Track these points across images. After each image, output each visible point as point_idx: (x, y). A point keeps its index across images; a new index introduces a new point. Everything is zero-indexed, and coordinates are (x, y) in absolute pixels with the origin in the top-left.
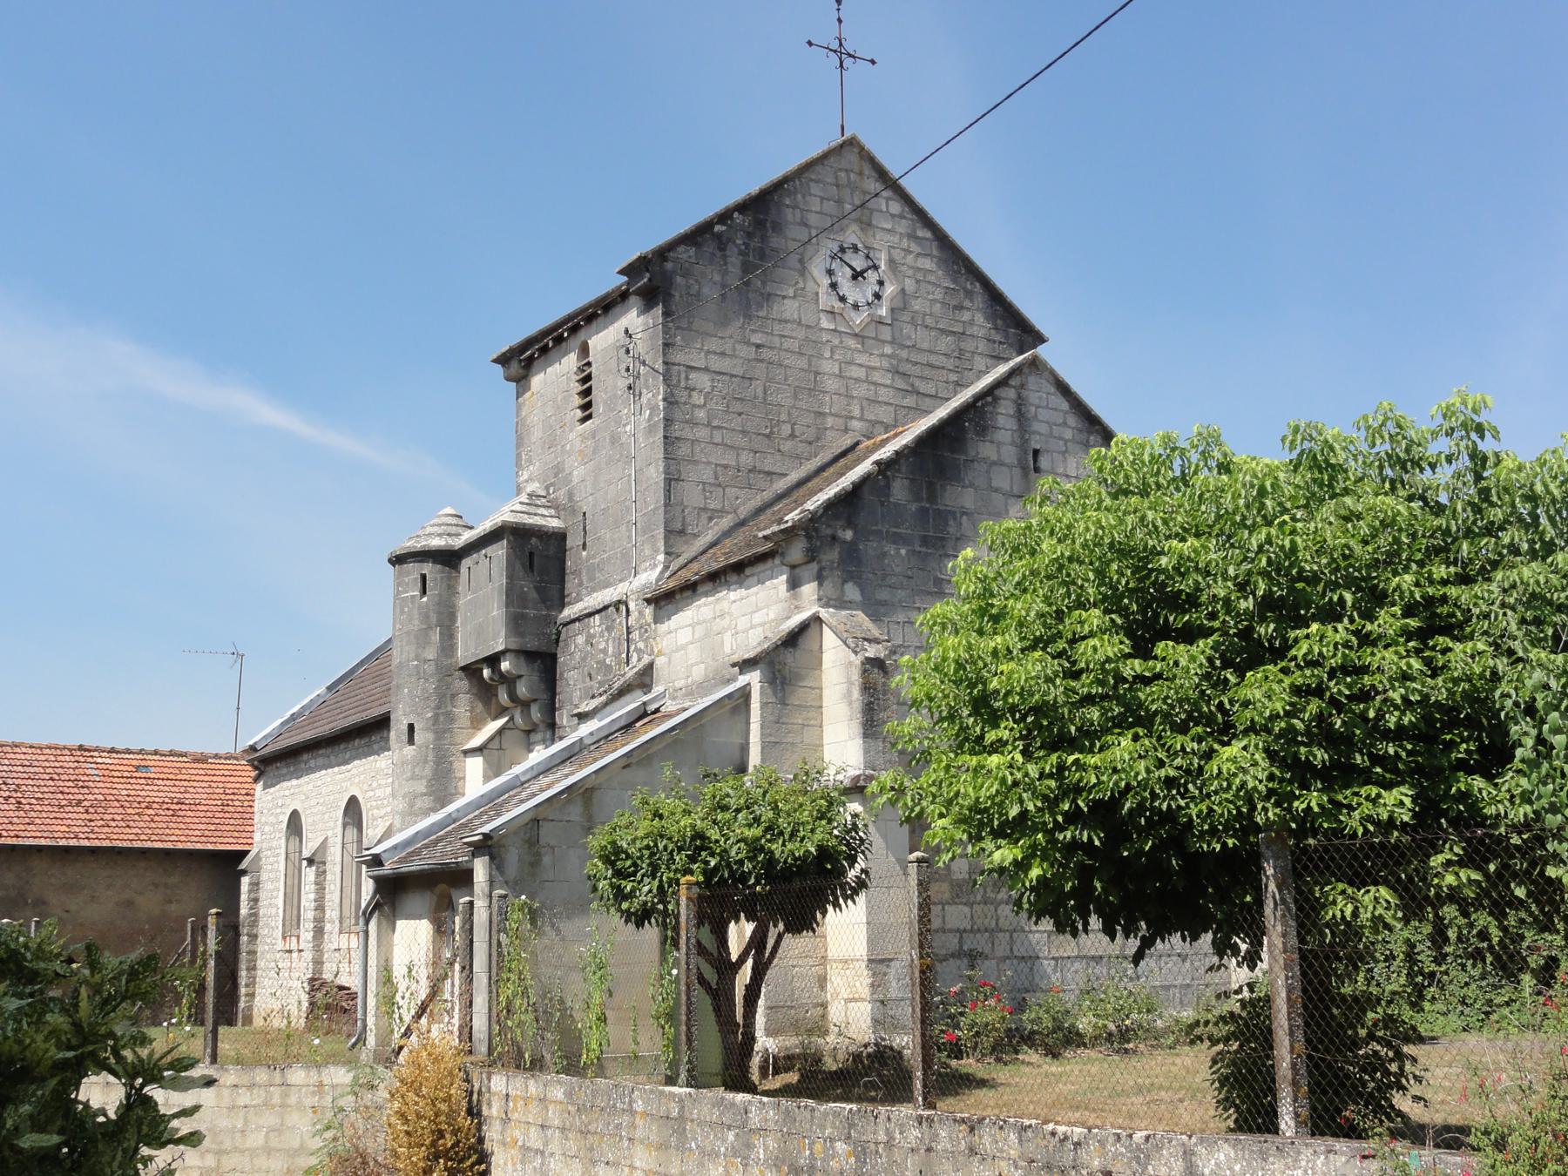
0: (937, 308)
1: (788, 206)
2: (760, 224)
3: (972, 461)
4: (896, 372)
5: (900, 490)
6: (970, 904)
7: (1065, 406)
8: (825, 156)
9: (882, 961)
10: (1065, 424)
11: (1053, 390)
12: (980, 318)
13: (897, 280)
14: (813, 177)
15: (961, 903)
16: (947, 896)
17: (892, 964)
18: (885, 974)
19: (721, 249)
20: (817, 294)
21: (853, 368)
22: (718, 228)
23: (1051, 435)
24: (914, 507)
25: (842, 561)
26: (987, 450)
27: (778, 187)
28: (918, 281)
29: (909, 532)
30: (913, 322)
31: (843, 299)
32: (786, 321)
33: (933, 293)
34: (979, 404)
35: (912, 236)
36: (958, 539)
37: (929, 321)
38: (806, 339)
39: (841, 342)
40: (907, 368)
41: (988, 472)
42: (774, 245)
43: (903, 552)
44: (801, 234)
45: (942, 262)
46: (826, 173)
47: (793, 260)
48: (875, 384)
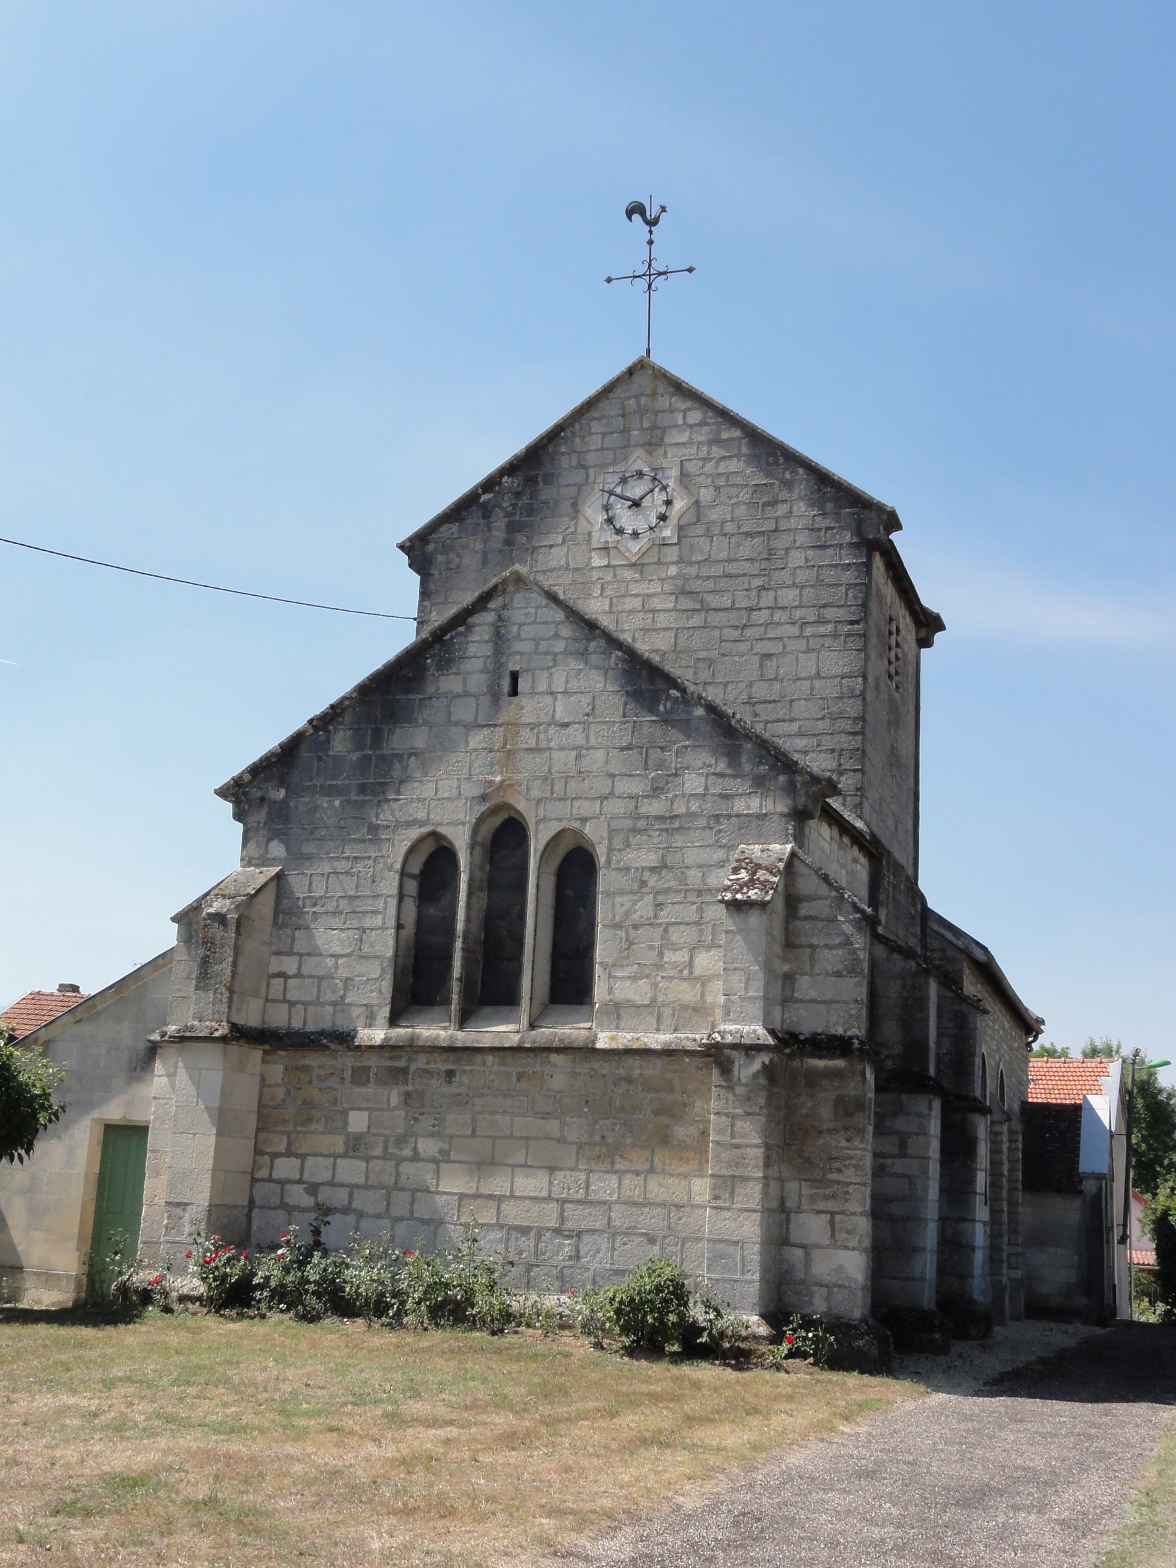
0: (742, 511)
1: (563, 454)
2: (531, 481)
3: (430, 698)
4: (682, 592)
5: (341, 742)
6: (367, 1159)
7: (560, 615)
8: (609, 390)
9: (179, 1205)
10: (557, 636)
11: (544, 602)
12: (801, 508)
13: (690, 493)
14: (596, 415)
15: (357, 1157)
16: (340, 1149)
17: (189, 1208)
18: (180, 1218)
19: (484, 517)
20: (590, 534)
21: (628, 600)
22: (484, 498)
23: (536, 651)
24: (354, 757)
25: (270, 819)
26: (450, 683)
27: (554, 435)
28: (718, 489)
29: (347, 782)
30: (709, 535)
31: (620, 531)
32: (551, 571)
33: (737, 496)
34: (448, 637)
35: (716, 441)
36: (402, 782)
37: (730, 528)
38: (574, 583)
39: (615, 575)
40: (696, 585)
41: (448, 706)
42: (543, 497)
43: (337, 803)
44: (578, 476)
45: (754, 459)
46: (610, 407)
47: (566, 507)
48: (653, 611)
